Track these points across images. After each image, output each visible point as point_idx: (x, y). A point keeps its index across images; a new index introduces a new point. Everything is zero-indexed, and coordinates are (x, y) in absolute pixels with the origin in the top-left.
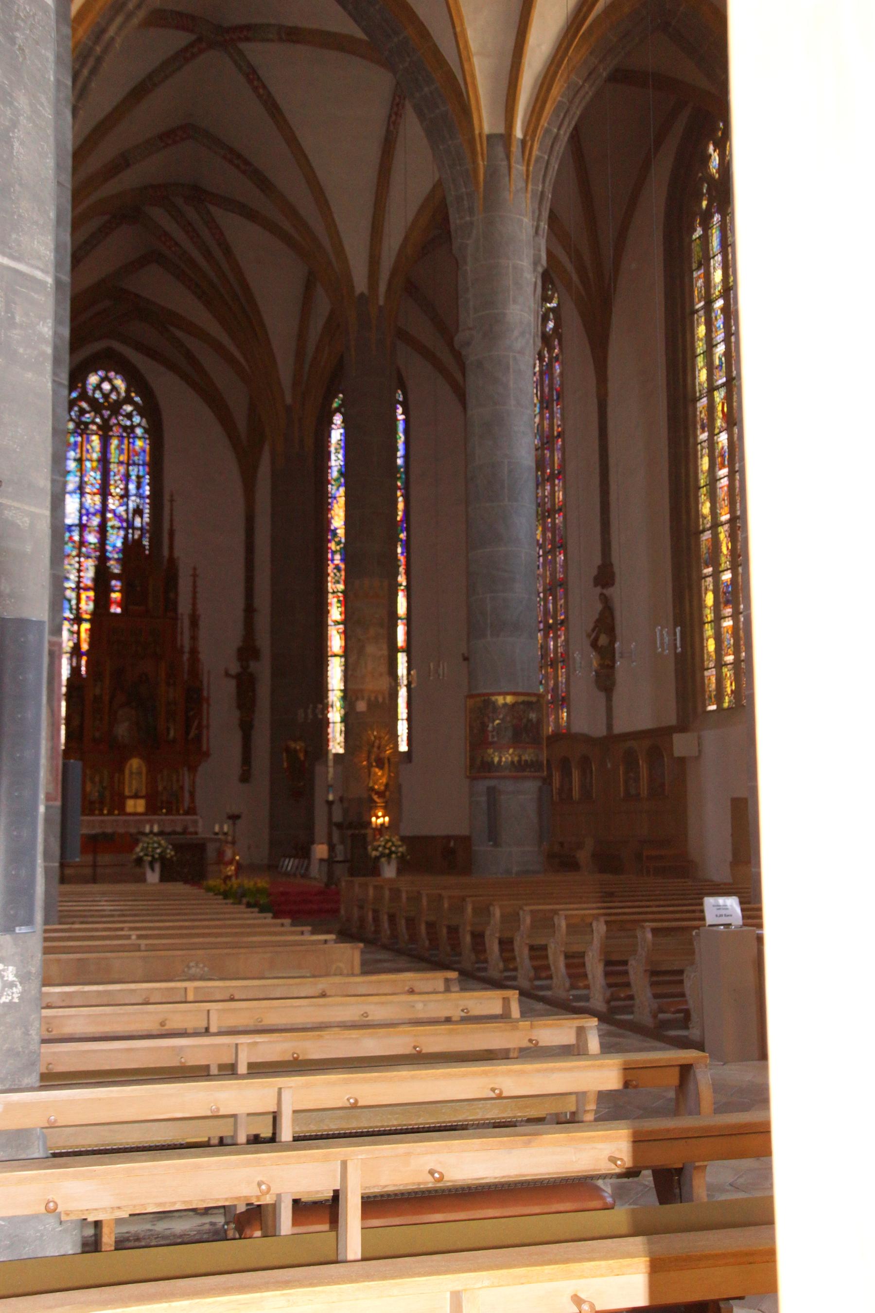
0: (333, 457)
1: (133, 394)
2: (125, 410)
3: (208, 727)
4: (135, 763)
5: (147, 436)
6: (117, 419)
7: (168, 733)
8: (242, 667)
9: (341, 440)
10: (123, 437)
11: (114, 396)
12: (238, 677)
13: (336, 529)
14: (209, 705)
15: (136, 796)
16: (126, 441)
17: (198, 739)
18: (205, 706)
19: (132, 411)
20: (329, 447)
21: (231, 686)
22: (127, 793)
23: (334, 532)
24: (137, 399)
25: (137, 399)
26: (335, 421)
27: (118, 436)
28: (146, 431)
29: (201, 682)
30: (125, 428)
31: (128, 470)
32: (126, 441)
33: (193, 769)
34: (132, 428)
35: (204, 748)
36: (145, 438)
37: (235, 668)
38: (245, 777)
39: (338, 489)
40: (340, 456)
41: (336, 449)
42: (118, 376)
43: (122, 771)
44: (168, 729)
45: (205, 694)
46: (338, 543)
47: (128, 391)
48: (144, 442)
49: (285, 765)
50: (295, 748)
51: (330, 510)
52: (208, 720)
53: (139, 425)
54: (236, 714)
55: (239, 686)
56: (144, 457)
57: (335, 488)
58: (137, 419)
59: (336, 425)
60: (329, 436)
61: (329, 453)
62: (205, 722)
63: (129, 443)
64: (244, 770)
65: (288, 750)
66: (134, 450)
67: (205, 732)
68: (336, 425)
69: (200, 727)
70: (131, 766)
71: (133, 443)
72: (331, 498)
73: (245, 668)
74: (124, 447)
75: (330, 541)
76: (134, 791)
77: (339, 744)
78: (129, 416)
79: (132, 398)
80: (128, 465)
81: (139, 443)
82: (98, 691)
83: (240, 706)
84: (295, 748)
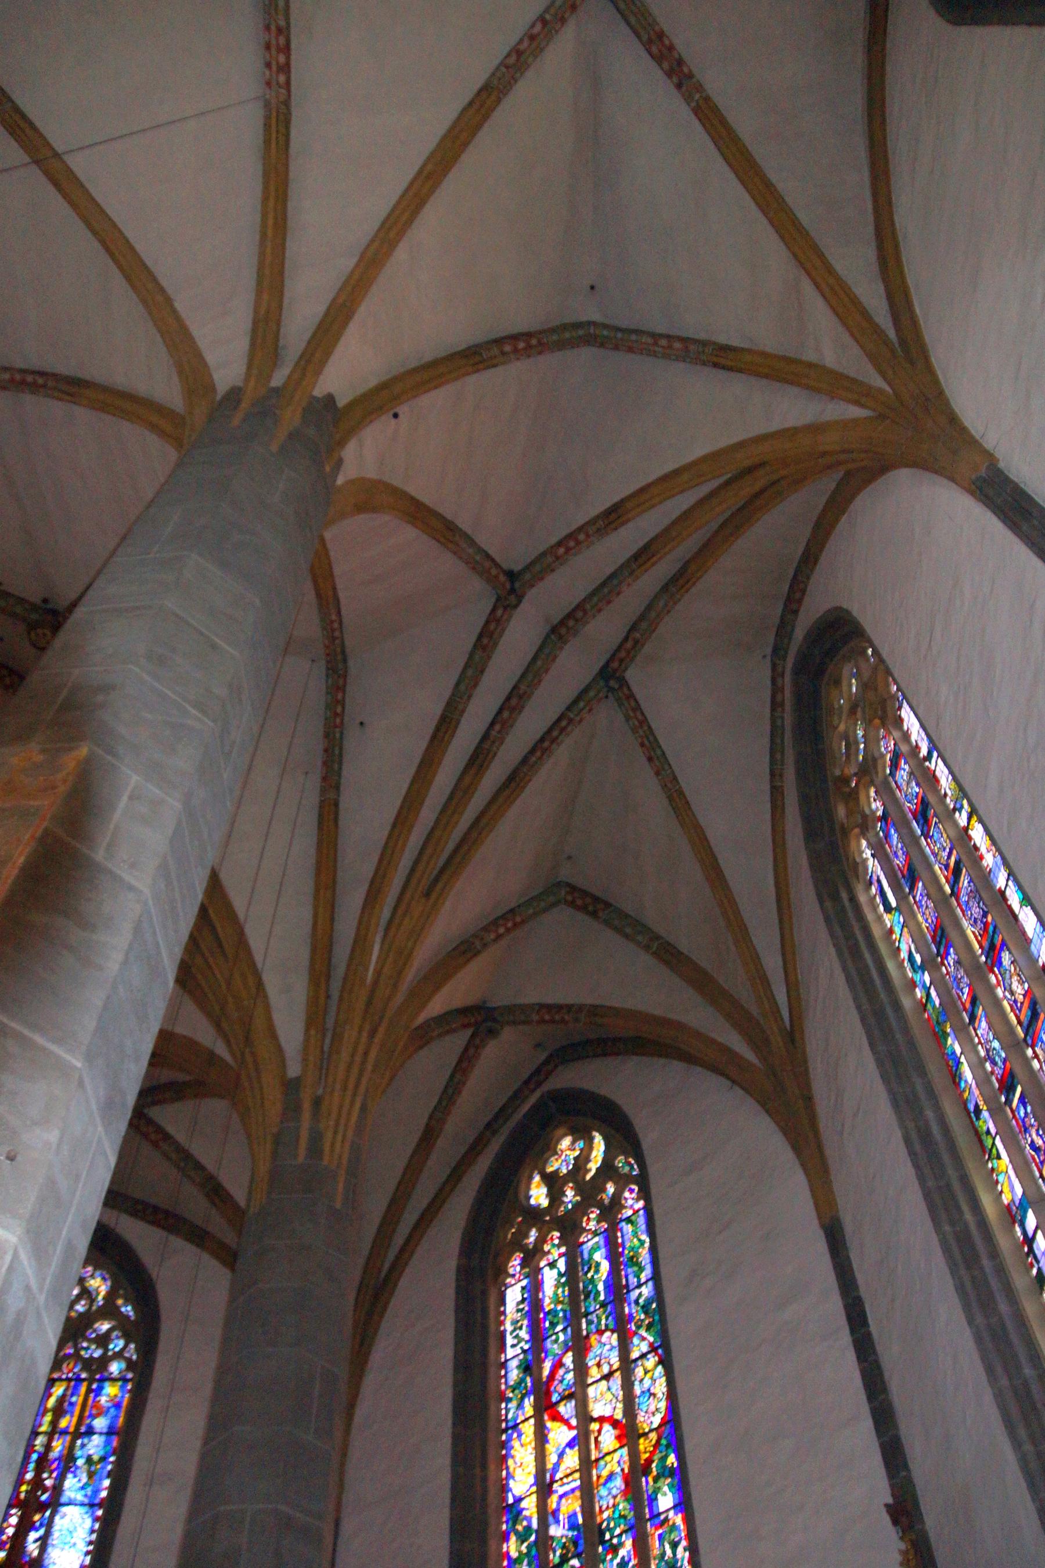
0: (510, 1340)
1: (120, 1302)
2: (95, 1331)
5: (130, 1375)
6: (75, 1346)
9: (523, 1300)
10: (79, 1380)
11: (80, 1308)
13: (519, 1500)
16: (83, 1389)
19: (109, 1331)
20: (503, 1323)
23: (514, 1511)
24: (128, 1310)
25: (128, 1310)
26: (511, 1271)
27: (69, 1380)
28: (131, 1365)
30: (88, 1364)
31: (72, 1447)
32: (83, 1389)
34: (104, 1362)
36: (125, 1380)
39: (520, 1406)
40: (524, 1334)
41: (515, 1322)
42: (98, 1273)
46: (522, 1538)
47: (110, 1297)
48: (122, 1387)
51: (504, 1459)
53: (119, 1355)
56: (117, 1417)
57: (513, 1405)
58: (117, 1345)
59: (513, 1276)
60: (503, 1302)
61: (502, 1336)
63: (89, 1391)
66: (96, 1404)
68: (513, 1276)
71: (98, 1392)
72: (505, 1431)
74: (77, 1399)
75: (506, 1537)
78: (103, 1340)
79: (118, 1308)
80: (77, 1435)
81: (111, 1390)
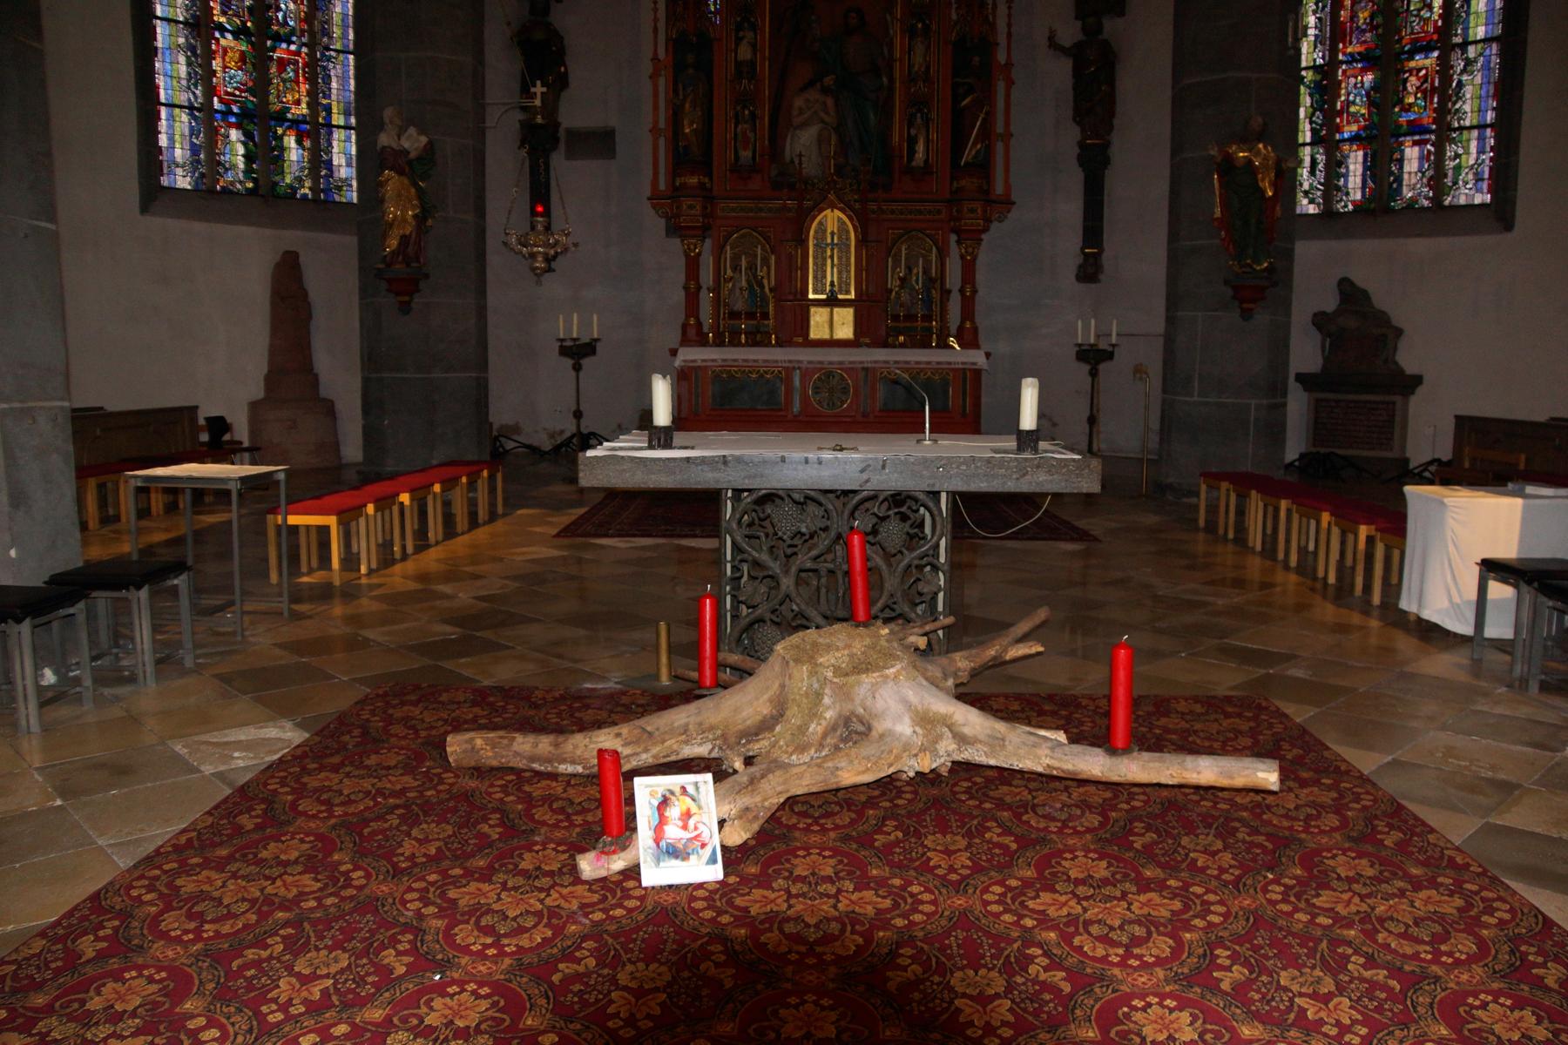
3: (1007, 136)
4: (832, 219)
7: (912, 152)
8: (1084, 30)
12: (1077, 54)
14: (1010, 83)
15: (832, 302)
17: (983, 167)
18: (1001, 86)
21: (1060, 72)
22: (811, 296)
29: (993, 26)
33: (970, 238)
35: (999, 189)
37: (1070, 33)
38: (1090, 271)
43: (803, 242)
44: (912, 142)
45: (1002, 57)
49: (1218, 213)
50: (1249, 162)
52: (1007, 123)
54: (1072, 134)
55: (1077, 71)
62: (1000, 128)
64: (1086, 255)
65: (1227, 167)
67: (1000, 147)
69: (986, 134)
70: (822, 228)
73: (1092, 32)
76: (828, 288)
77: (1306, 193)
82: (745, 53)
83: (1079, 115)
84: (1249, 162)
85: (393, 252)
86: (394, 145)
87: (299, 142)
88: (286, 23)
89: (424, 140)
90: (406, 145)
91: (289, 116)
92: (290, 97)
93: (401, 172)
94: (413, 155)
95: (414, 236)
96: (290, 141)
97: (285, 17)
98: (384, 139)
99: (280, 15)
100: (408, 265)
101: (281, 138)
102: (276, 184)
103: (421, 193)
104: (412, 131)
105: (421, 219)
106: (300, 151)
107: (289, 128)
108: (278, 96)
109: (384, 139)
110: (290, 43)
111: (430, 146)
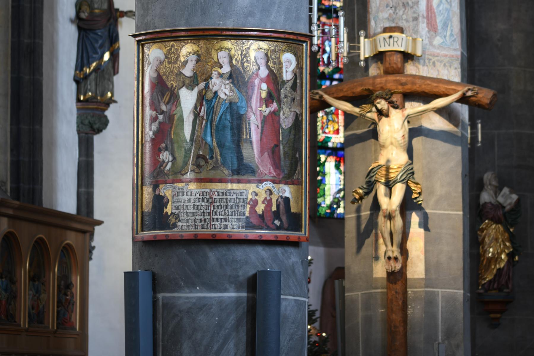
85: (490, 281)
86: (493, 201)
87: (337, 167)
88: (329, 63)
89: (515, 197)
90: (500, 199)
91: (330, 145)
92: (331, 128)
93: (497, 222)
94: (508, 208)
95: (505, 269)
96: (330, 165)
97: (329, 58)
98: (486, 197)
99: (325, 57)
100: (500, 290)
101: (323, 164)
102: (319, 205)
103: (512, 238)
104: (506, 190)
105: (510, 256)
106: (338, 175)
107: (329, 155)
108: (322, 128)
109: (486, 197)
110: (332, 80)
111: (518, 201)
